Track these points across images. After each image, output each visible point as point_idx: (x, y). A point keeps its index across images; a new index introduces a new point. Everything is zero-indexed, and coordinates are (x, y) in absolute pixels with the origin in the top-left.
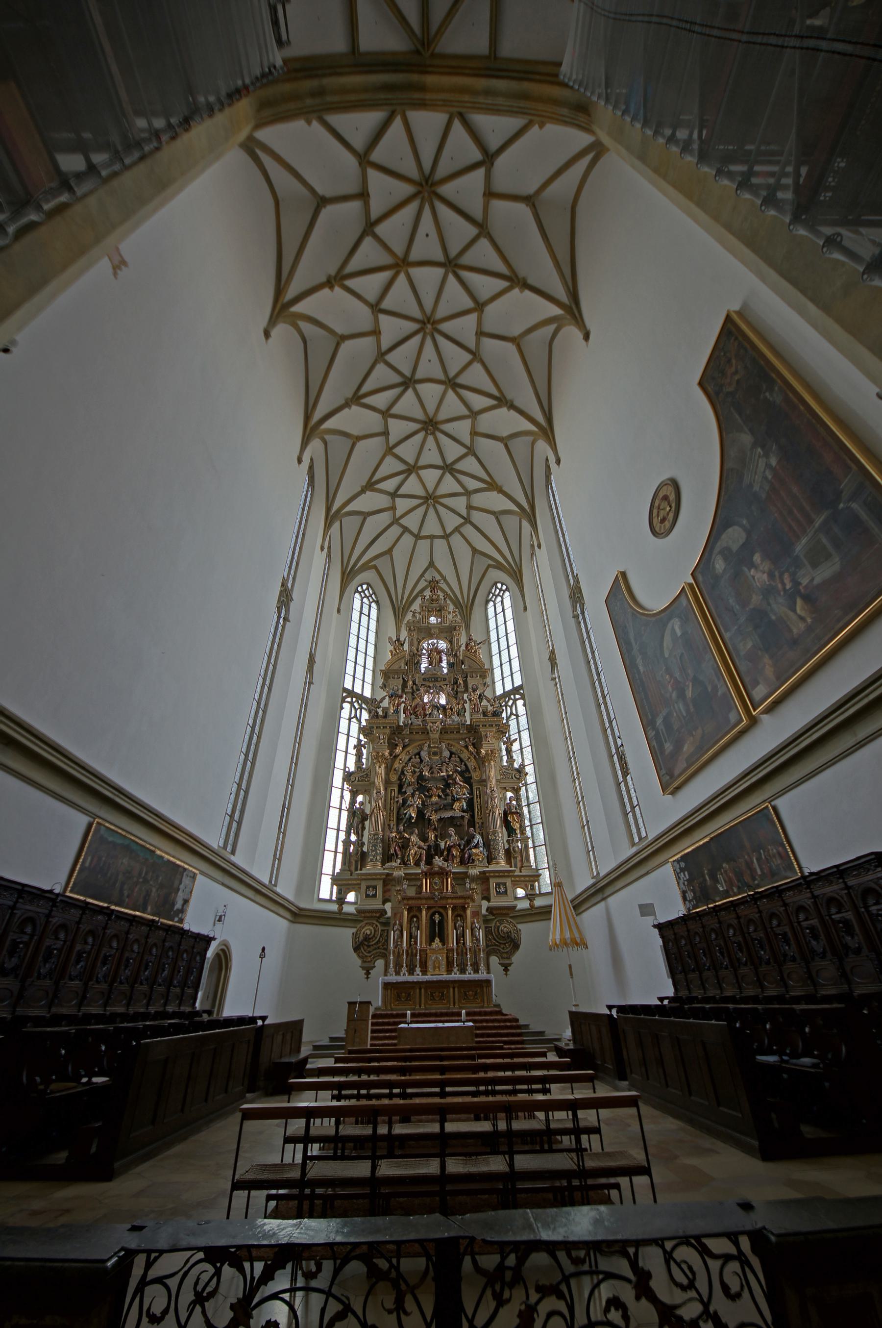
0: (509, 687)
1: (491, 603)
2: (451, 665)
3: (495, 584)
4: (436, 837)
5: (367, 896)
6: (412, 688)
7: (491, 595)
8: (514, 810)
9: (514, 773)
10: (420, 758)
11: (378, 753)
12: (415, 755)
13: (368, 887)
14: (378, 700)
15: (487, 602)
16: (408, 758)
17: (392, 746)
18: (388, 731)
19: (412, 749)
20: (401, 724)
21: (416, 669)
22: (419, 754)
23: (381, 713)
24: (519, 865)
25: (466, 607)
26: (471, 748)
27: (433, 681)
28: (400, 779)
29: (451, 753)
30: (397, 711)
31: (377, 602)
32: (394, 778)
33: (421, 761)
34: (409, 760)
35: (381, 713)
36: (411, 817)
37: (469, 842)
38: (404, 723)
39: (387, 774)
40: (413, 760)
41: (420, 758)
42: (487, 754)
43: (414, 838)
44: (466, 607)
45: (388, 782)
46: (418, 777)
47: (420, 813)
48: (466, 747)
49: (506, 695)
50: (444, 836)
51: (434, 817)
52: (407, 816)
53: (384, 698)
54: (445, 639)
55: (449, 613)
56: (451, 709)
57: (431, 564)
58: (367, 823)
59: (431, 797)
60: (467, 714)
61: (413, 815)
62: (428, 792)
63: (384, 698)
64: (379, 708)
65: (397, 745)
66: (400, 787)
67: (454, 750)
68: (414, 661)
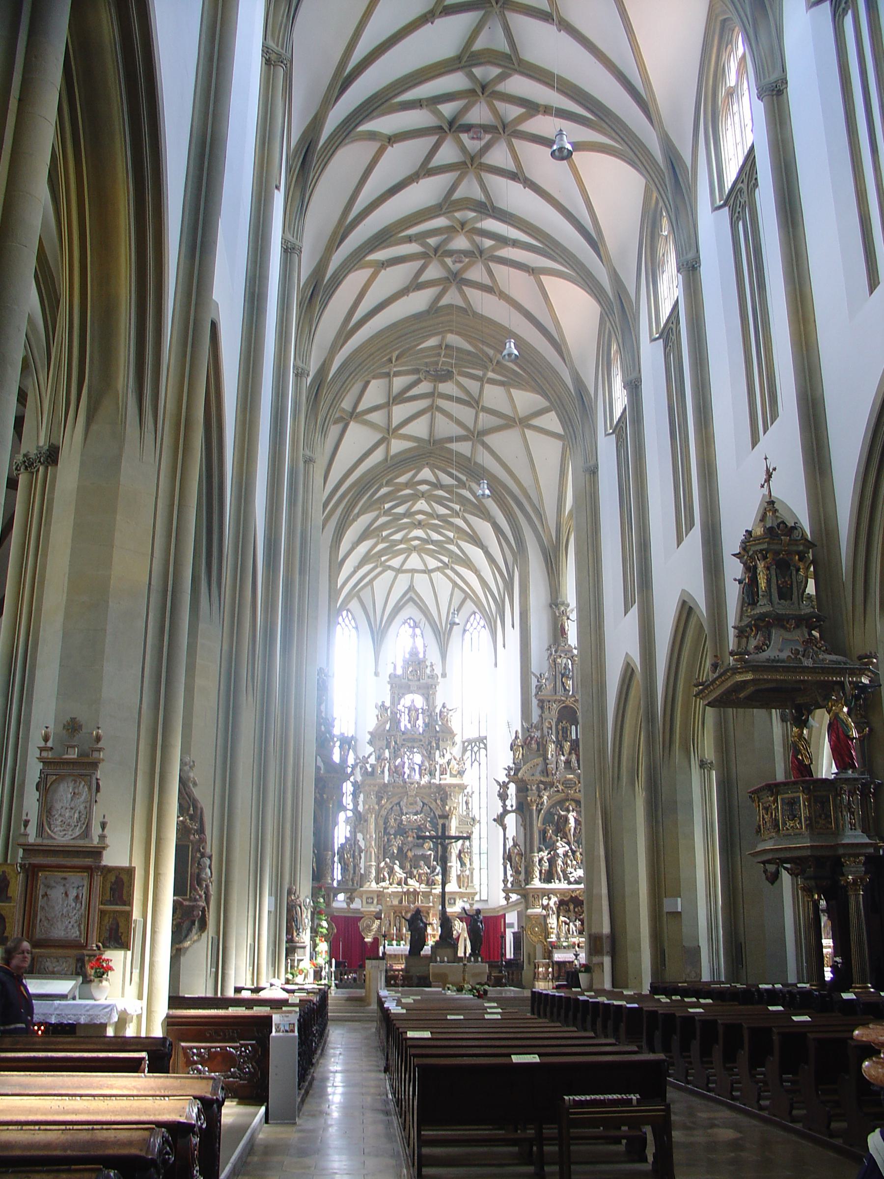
0: (475, 735)
1: (467, 633)
2: (427, 725)
3: (474, 613)
4: (411, 866)
5: (367, 903)
6: (394, 748)
7: (469, 625)
8: (466, 850)
9: (469, 820)
10: (400, 806)
11: (370, 806)
12: (396, 804)
13: (367, 898)
14: (366, 756)
15: (465, 631)
16: (390, 807)
17: (379, 799)
18: (376, 789)
19: (395, 800)
20: (386, 782)
21: (397, 728)
22: (399, 803)
23: (370, 769)
24: (466, 885)
25: (444, 634)
26: (439, 801)
27: (410, 741)
28: (385, 823)
29: (424, 804)
30: (383, 772)
31: (357, 628)
32: (381, 822)
33: (401, 809)
34: (392, 808)
35: (370, 769)
36: (394, 852)
37: (433, 872)
38: (388, 781)
39: (376, 819)
40: (395, 808)
41: (400, 806)
42: (450, 809)
43: (397, 868)
44: (444, 634)
45: (376, 824)
46: (399, 823)
47: (400, 849)
48: (435, 801)
49: (470, 742)
50: (417, 866)
51: (410, 854)
52: (391, 851)
53: (371, 754)
54: (423, 695)
55: (427, 667)
56: (425, 770)
57: (411, 588)
58: (363, 855)
59: (407, 837)
60: (437, 773)
61: (395, 851)
62: (405, 833)
63: (371, 754)
64: (368, 763)
65: (382, 797)
66: (385, 829)
67: (426, 801)
68: (395, 722)
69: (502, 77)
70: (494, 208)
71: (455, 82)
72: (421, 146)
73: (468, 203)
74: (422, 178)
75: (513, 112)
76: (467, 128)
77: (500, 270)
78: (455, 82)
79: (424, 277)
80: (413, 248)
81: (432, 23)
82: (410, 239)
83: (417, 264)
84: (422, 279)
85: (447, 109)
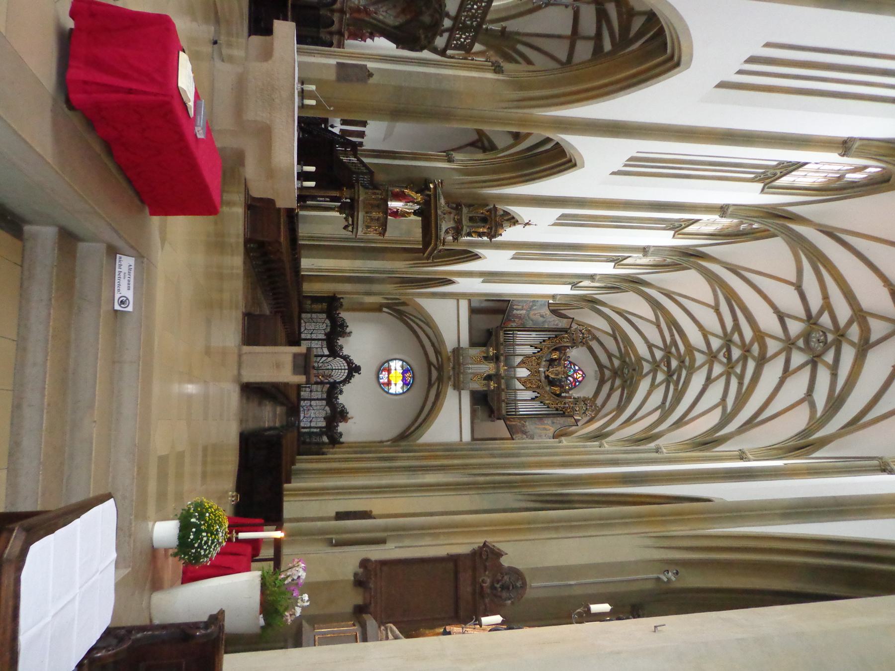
69: (754, 358)
70: (692, 374)
71: (748, 334)
72: (717, 329)
73: (693, 360)
74: (702, 333)
75: (738, 370)
76: (729, 351)
77: (662, 388)
78: (748, 334)
79: (655, 351)
80: (668, 339)
81: (774, 313)
82: (672, 335)
83: (661, 345)
84: (654, 348)
85: (736, 337)
